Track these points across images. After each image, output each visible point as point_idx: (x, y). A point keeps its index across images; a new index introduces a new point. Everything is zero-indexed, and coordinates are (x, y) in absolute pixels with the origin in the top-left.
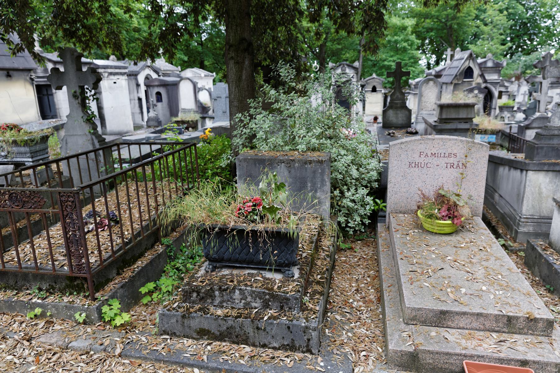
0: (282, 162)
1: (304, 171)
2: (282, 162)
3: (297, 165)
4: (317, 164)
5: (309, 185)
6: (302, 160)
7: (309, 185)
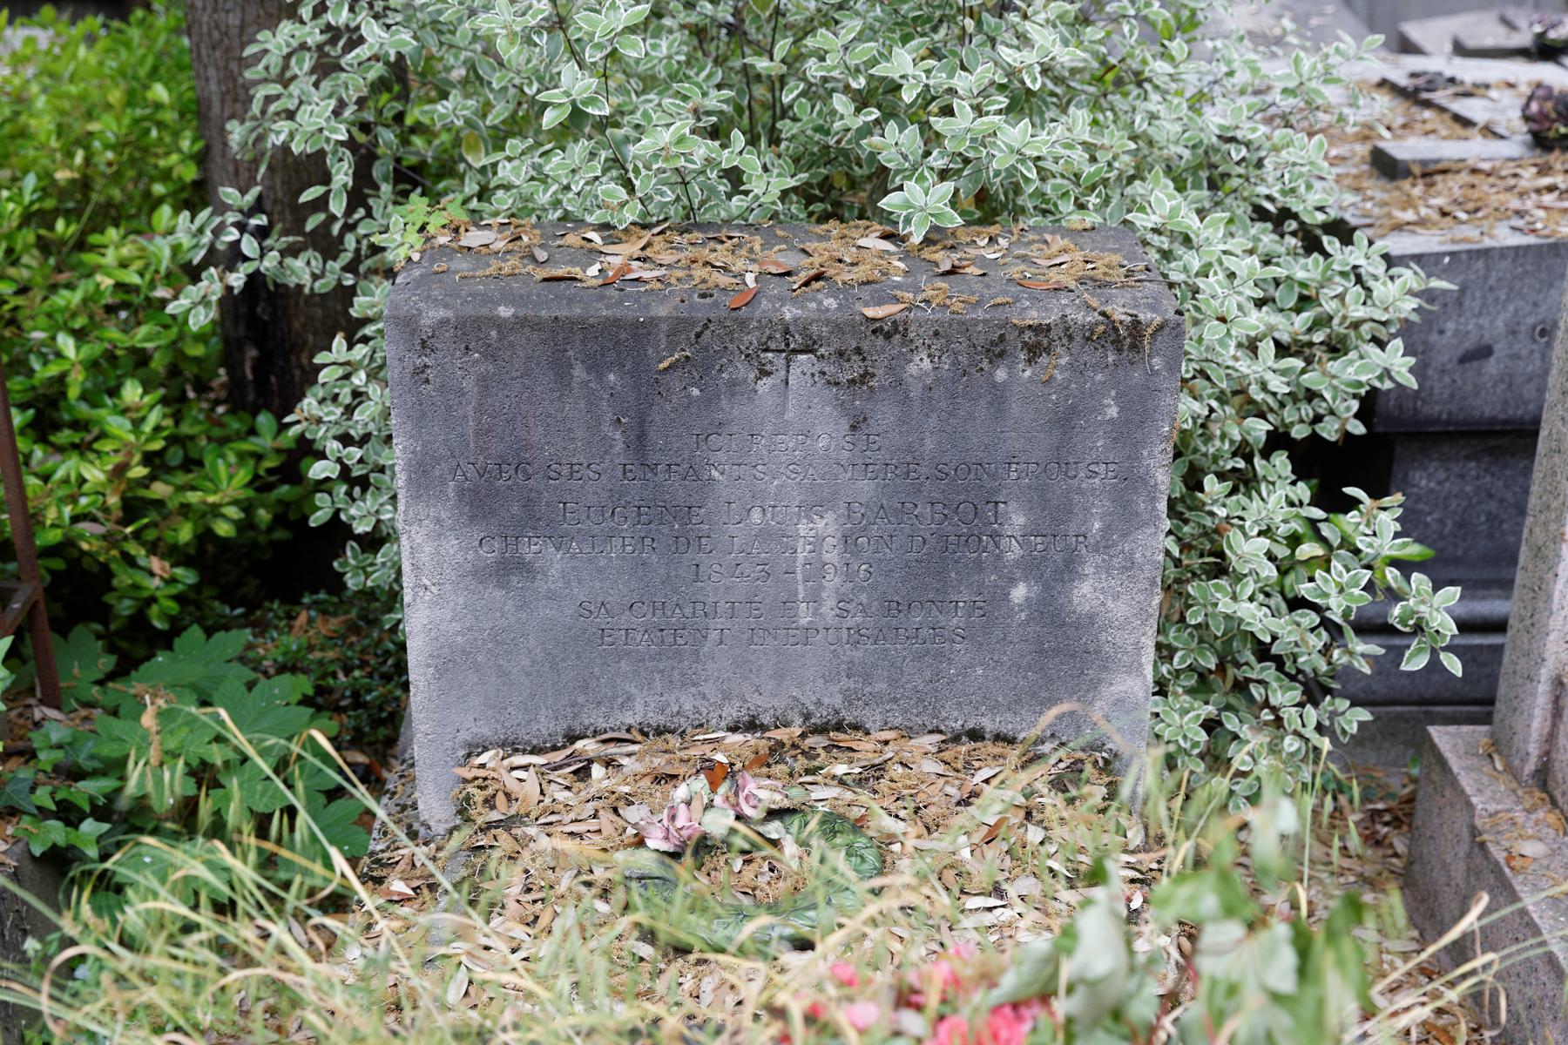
0: (796, 342)
1: (982, 410)
2: (796, 342)
3: (921, 364)
4: (1089, 356)
5: (1018, 520)
6: (966, 327)
7: (1018, 520)
